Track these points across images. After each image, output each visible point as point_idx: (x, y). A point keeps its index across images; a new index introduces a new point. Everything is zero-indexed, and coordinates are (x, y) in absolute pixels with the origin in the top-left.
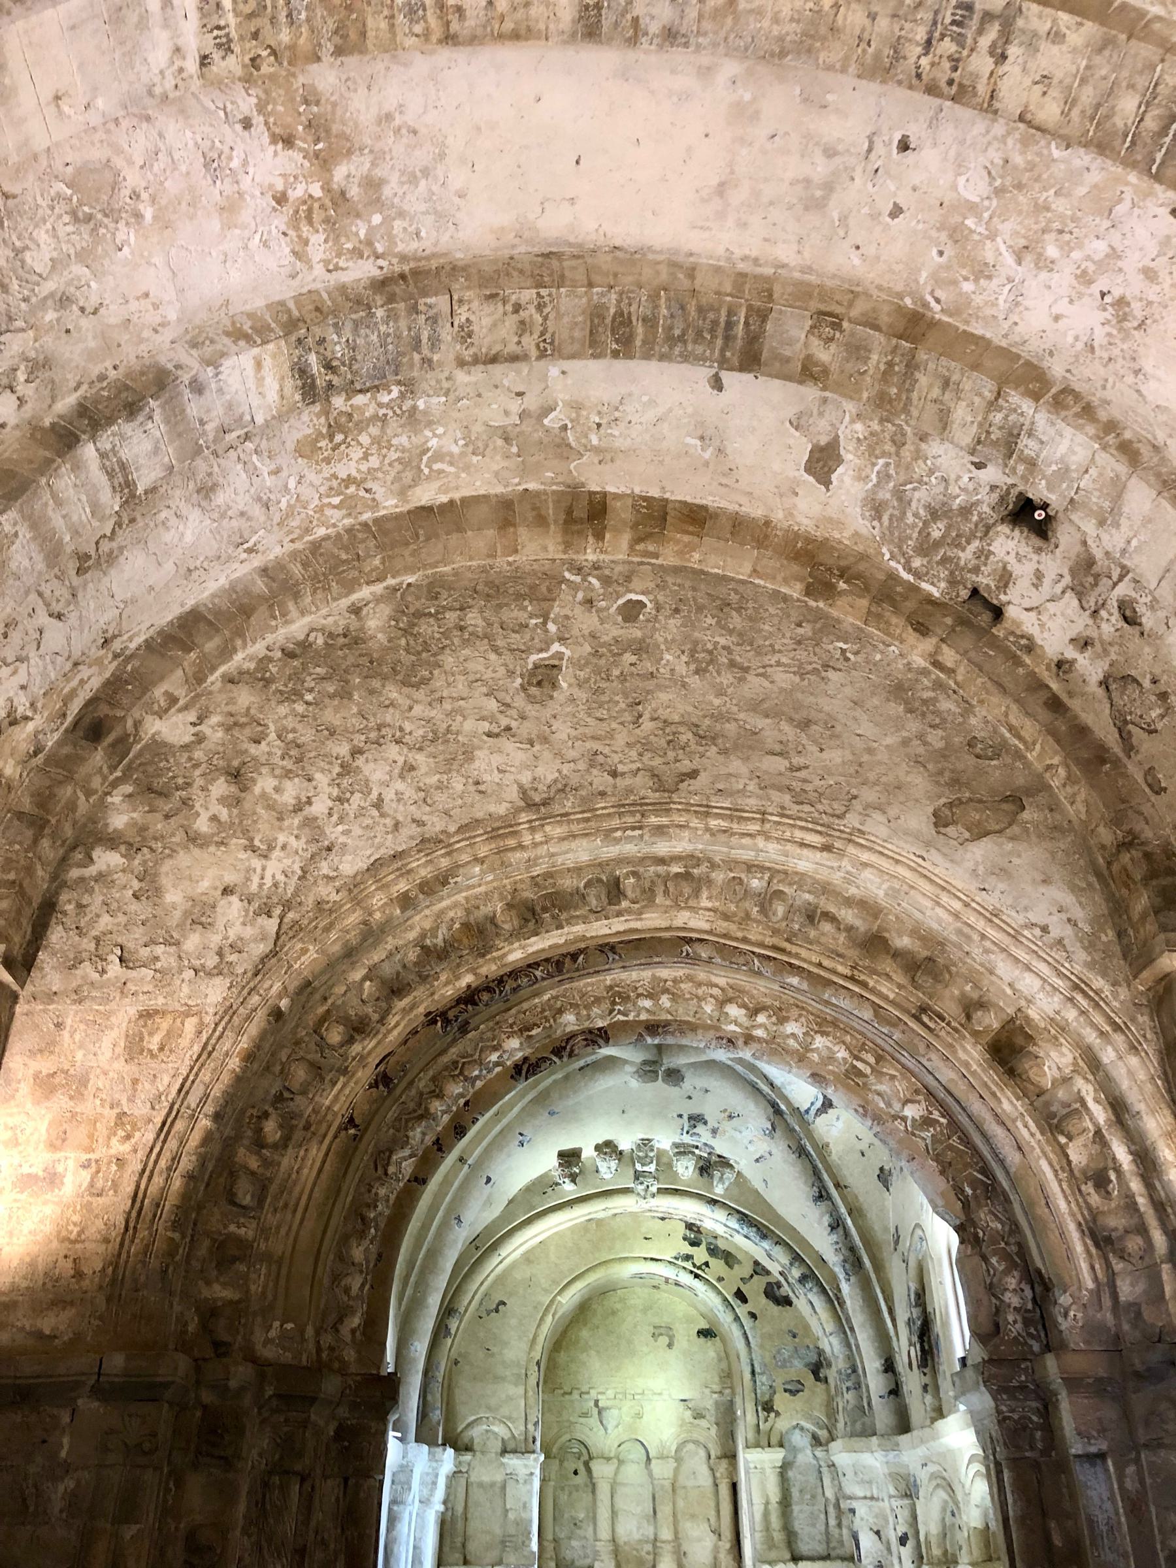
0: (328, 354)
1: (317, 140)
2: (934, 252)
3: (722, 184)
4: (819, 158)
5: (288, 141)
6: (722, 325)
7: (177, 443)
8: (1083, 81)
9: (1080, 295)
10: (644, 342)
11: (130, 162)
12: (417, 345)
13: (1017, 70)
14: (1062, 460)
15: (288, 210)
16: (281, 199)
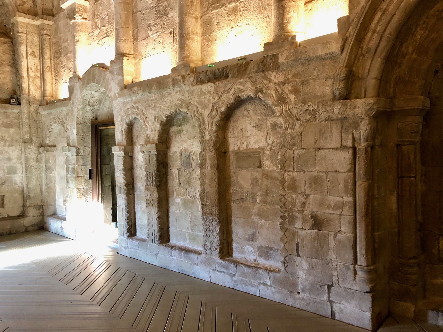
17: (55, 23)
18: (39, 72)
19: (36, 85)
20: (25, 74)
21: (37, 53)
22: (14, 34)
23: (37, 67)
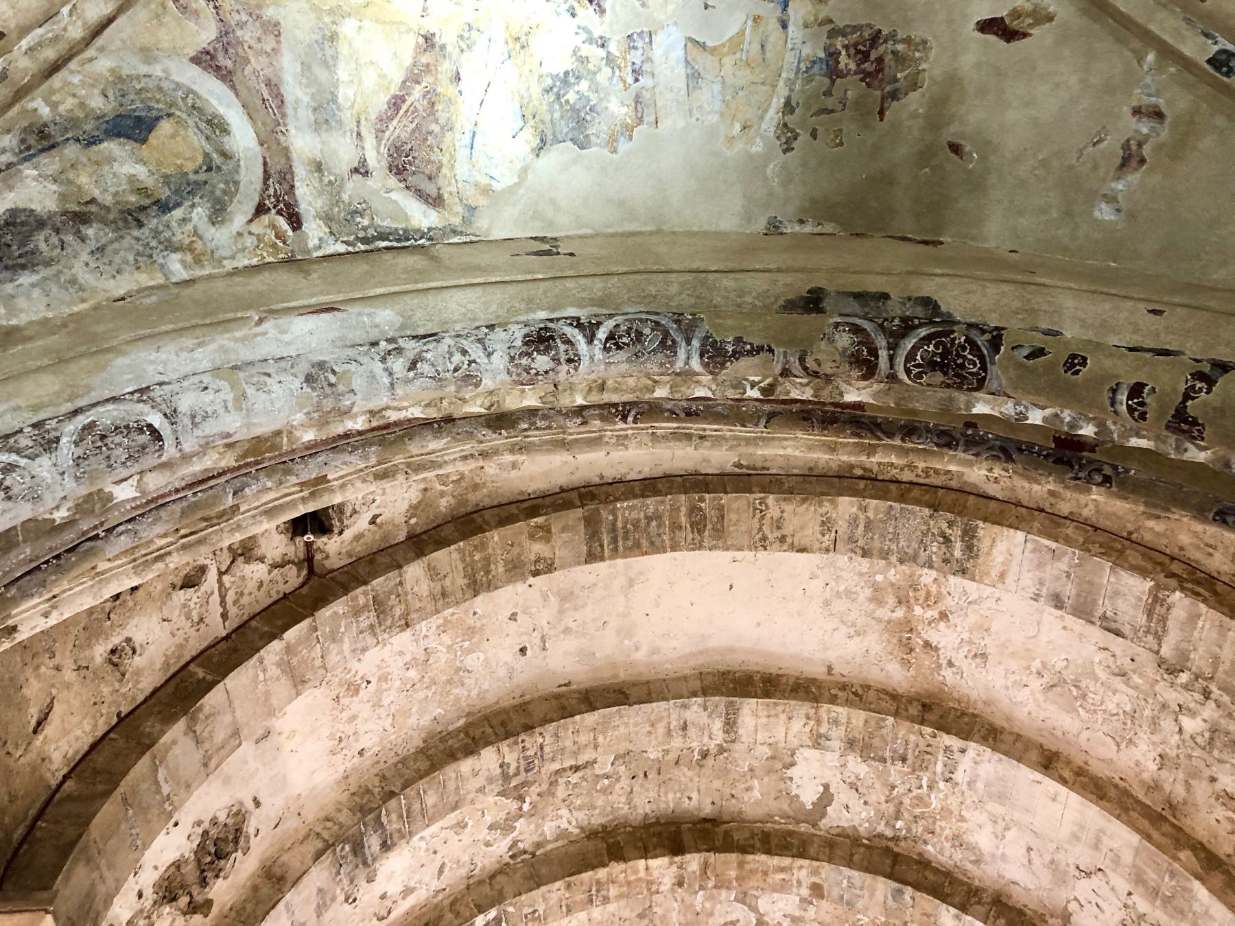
0: (944, 549)
1: (909, 638)
2: (479, 612)
4: (573, 625)
5: (927, 644)
6: (620, 539)
7: (1097, 580)
10: (678, 509)
11: (1033, 693)
12: (869, 525)
14: (341, 640)
15: (941, 607)
16: (944, 616)
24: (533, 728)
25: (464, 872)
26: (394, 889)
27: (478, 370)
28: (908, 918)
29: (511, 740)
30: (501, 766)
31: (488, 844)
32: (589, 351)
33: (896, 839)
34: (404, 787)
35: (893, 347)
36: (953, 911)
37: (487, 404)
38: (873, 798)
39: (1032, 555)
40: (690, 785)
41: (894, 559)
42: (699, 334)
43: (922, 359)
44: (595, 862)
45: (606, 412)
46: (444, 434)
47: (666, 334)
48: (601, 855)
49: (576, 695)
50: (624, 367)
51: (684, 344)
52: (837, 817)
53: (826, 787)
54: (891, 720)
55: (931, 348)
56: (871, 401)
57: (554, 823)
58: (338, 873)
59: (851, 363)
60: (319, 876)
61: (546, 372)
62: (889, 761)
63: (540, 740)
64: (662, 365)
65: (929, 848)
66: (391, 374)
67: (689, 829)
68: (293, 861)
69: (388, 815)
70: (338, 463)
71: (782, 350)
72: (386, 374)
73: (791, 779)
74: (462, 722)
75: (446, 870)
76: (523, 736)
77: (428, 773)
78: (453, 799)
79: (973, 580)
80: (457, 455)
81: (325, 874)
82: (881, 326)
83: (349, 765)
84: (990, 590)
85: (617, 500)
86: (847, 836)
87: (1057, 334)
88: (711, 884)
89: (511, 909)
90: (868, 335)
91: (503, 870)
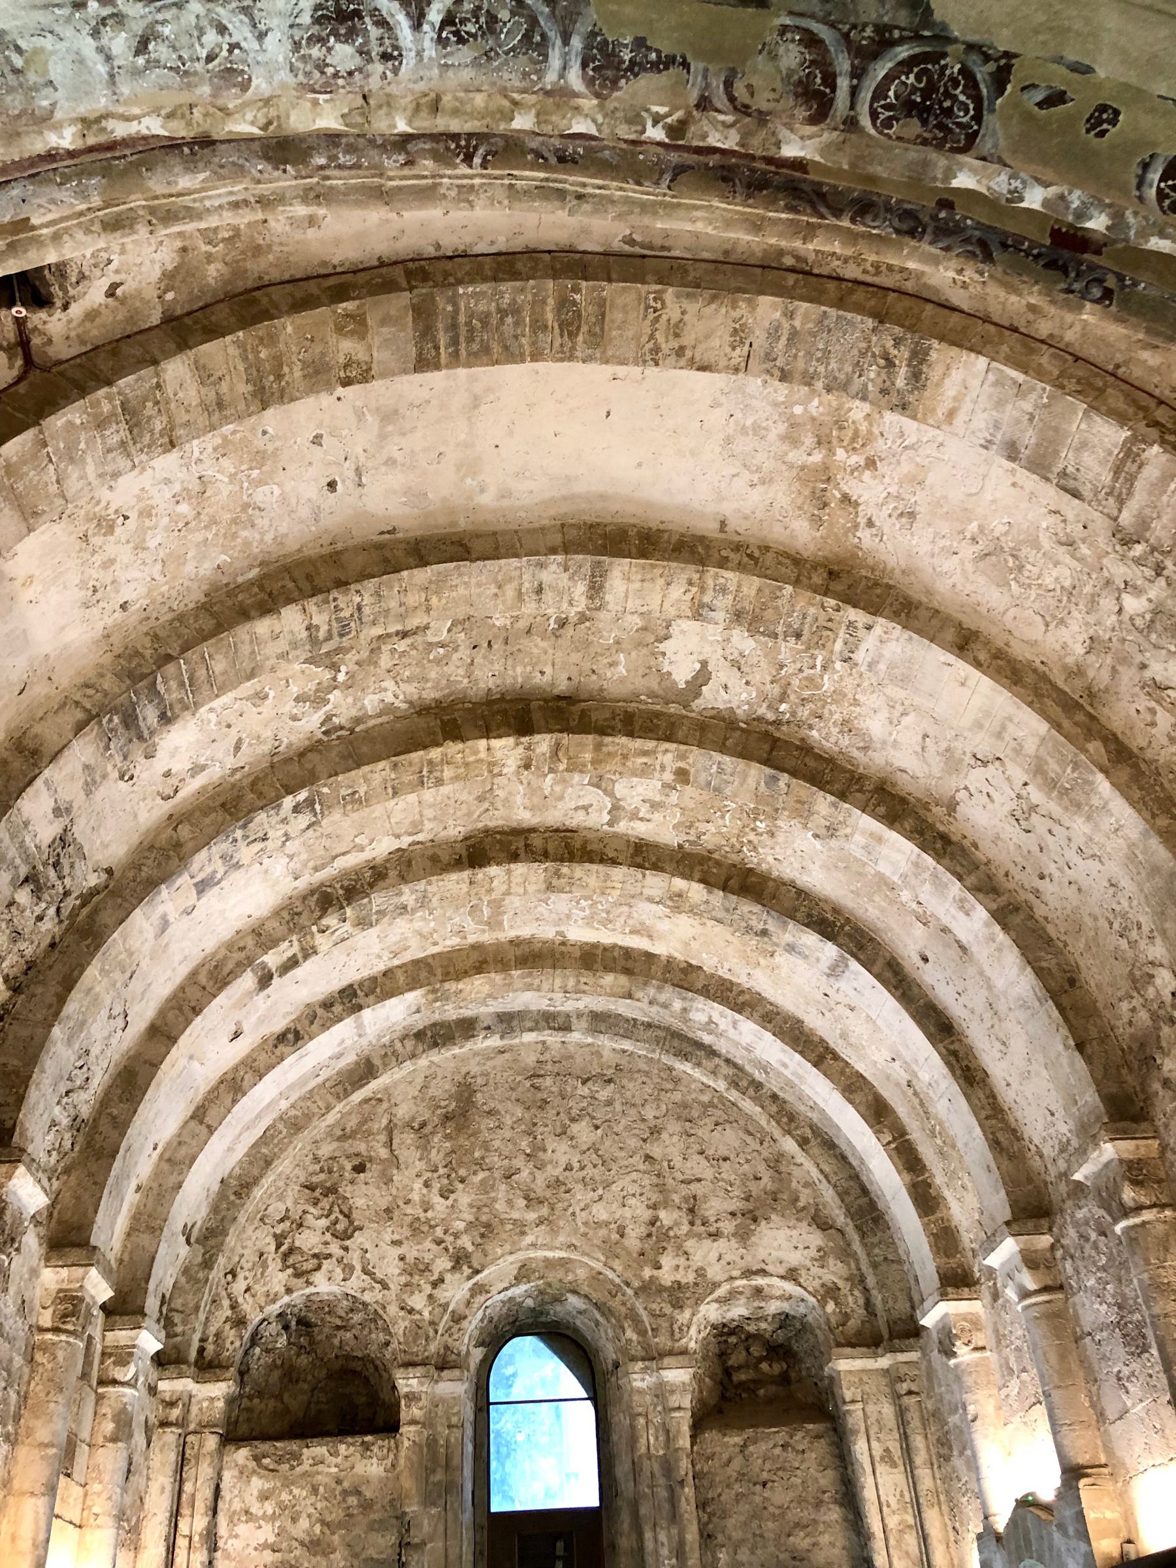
0: (884, 376)
1: (824, 490)
2: (270, 430)
3: (476, 407)
4: (398, 456)
5: (846, 498)
6: (462, 339)
8: (253, 652)
9: (139, 499)
10: (544, 302)
11: (962, 562)
12: (794, 334)
13: (296, 629)
14: (83, 460)
15: (870, 451)
16: (871, 463)
17: (924, 1355)
18: (910, 1510)
19: (907, 1553)
20: (875, 1526)
21: (897, 1453)
22: (836, 1406)
23: (902, 1495)
24: (347, 583)
25: (266, 748)
26: (180, 765)
27: (244, 61)
28: (780, 805)
29: (320, 597)
30: (308, 629)
31: (295, 718)
32: (416, 41)
33: (777, 723)
34: (185, 648)
35: (858, 74)
36: (830, 798)
37: (262, 121)
38: (756, 678)
39: (992, 389)
40: (543, 657)
41: (819, 385)
42: (582, 27)
43: (897, 97)
44: (427, 741)
45: (441, 147)
46: (201, 165)
47: (533, 22)
48: (434, 733)
49: (403, 546)
50: (467, 74)
51: (559, 42)
52: (712, 698)
53: (704, 664)
54: (789, 589)
55: (911, 79)
56: (818, 158)
57: (377, 697)
58: (107, 748)
59: (797, 95)
60: (82, 751)
61: (350, 74)
62: (781, 637)
63: (358, 599)
64: (525, 75)
65: (814, 733)
66: (109, 58)
67: (540, 707)
68: (49, 732)
69: (165, 682)
70: (42, 201)
71: (701, 65)
72: (99, 58)
73: (664, 654)
74: (254, 573)
75: (244, 747)
76: (334, 594)
77: (213, 634)
78: (247, 665)
79: (914, 418)
80: (224, 200)
81: (91, 749)
82: (846, 36)
83: (110, 622)
84: (933, 432)
85: (460, 282)
86: (723, 719)
87: (1088, 70)
88: (562, 767)
89: (325, 790)
90: (827, 51)
91: (314, 748)
